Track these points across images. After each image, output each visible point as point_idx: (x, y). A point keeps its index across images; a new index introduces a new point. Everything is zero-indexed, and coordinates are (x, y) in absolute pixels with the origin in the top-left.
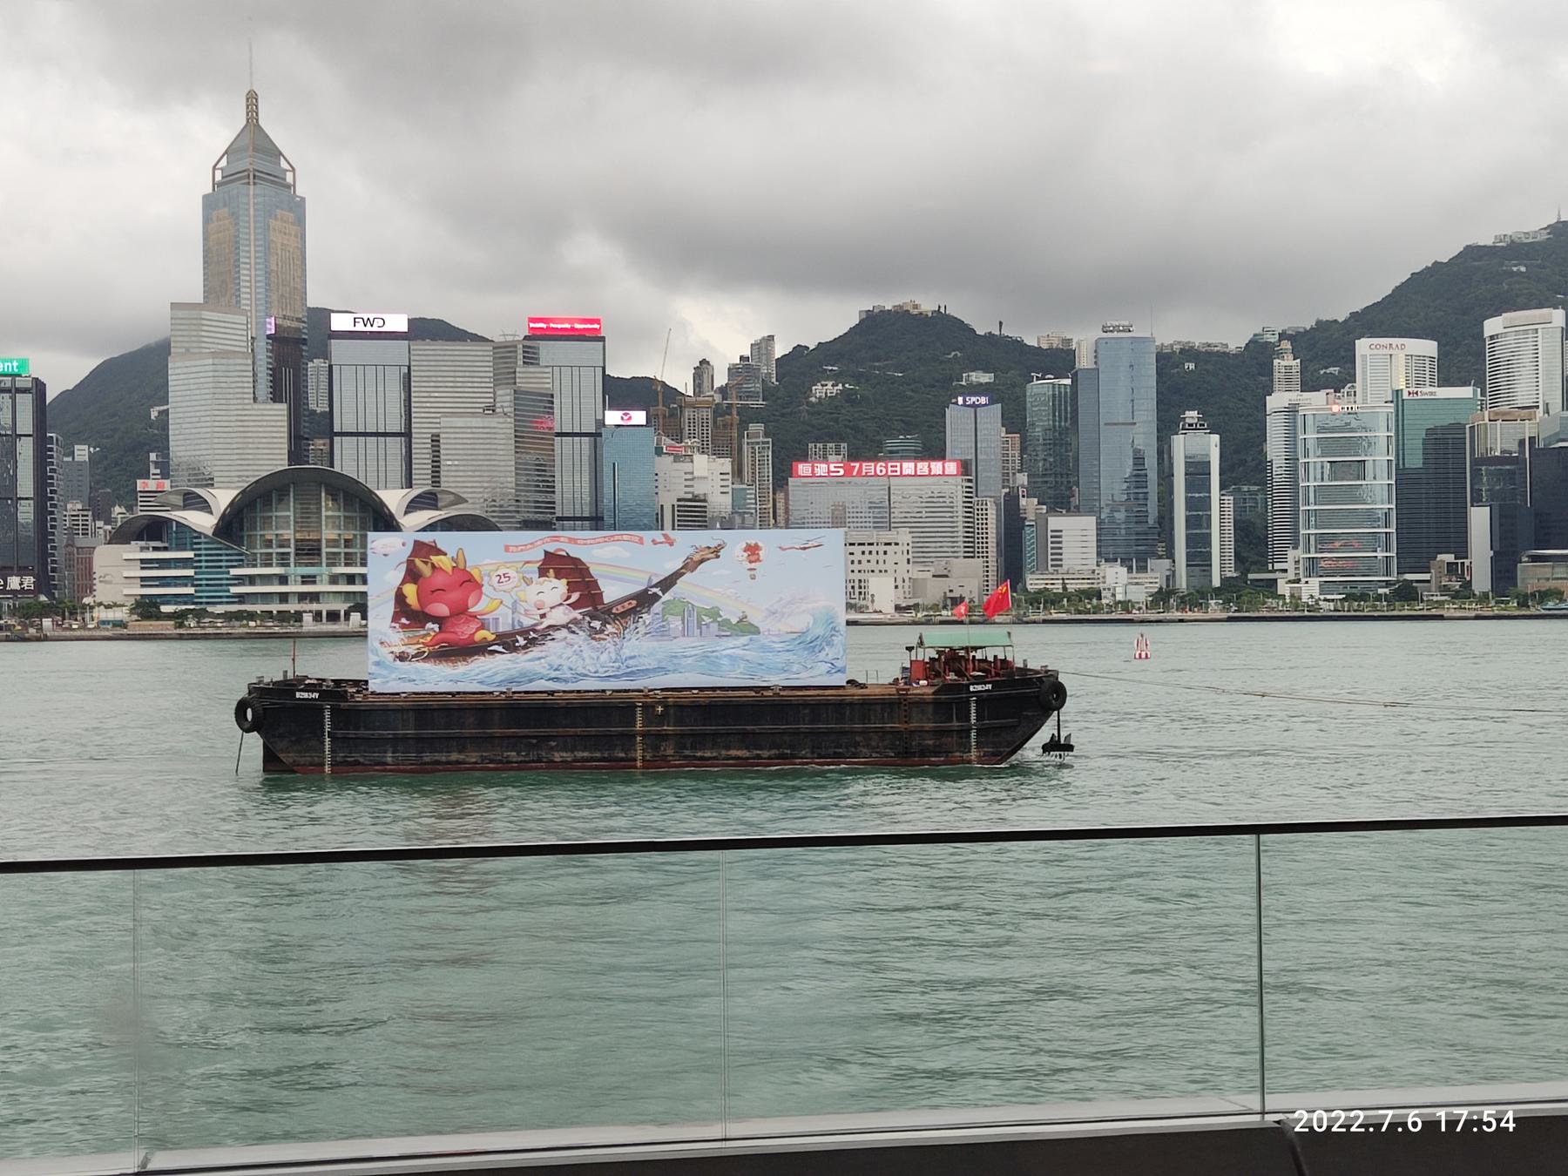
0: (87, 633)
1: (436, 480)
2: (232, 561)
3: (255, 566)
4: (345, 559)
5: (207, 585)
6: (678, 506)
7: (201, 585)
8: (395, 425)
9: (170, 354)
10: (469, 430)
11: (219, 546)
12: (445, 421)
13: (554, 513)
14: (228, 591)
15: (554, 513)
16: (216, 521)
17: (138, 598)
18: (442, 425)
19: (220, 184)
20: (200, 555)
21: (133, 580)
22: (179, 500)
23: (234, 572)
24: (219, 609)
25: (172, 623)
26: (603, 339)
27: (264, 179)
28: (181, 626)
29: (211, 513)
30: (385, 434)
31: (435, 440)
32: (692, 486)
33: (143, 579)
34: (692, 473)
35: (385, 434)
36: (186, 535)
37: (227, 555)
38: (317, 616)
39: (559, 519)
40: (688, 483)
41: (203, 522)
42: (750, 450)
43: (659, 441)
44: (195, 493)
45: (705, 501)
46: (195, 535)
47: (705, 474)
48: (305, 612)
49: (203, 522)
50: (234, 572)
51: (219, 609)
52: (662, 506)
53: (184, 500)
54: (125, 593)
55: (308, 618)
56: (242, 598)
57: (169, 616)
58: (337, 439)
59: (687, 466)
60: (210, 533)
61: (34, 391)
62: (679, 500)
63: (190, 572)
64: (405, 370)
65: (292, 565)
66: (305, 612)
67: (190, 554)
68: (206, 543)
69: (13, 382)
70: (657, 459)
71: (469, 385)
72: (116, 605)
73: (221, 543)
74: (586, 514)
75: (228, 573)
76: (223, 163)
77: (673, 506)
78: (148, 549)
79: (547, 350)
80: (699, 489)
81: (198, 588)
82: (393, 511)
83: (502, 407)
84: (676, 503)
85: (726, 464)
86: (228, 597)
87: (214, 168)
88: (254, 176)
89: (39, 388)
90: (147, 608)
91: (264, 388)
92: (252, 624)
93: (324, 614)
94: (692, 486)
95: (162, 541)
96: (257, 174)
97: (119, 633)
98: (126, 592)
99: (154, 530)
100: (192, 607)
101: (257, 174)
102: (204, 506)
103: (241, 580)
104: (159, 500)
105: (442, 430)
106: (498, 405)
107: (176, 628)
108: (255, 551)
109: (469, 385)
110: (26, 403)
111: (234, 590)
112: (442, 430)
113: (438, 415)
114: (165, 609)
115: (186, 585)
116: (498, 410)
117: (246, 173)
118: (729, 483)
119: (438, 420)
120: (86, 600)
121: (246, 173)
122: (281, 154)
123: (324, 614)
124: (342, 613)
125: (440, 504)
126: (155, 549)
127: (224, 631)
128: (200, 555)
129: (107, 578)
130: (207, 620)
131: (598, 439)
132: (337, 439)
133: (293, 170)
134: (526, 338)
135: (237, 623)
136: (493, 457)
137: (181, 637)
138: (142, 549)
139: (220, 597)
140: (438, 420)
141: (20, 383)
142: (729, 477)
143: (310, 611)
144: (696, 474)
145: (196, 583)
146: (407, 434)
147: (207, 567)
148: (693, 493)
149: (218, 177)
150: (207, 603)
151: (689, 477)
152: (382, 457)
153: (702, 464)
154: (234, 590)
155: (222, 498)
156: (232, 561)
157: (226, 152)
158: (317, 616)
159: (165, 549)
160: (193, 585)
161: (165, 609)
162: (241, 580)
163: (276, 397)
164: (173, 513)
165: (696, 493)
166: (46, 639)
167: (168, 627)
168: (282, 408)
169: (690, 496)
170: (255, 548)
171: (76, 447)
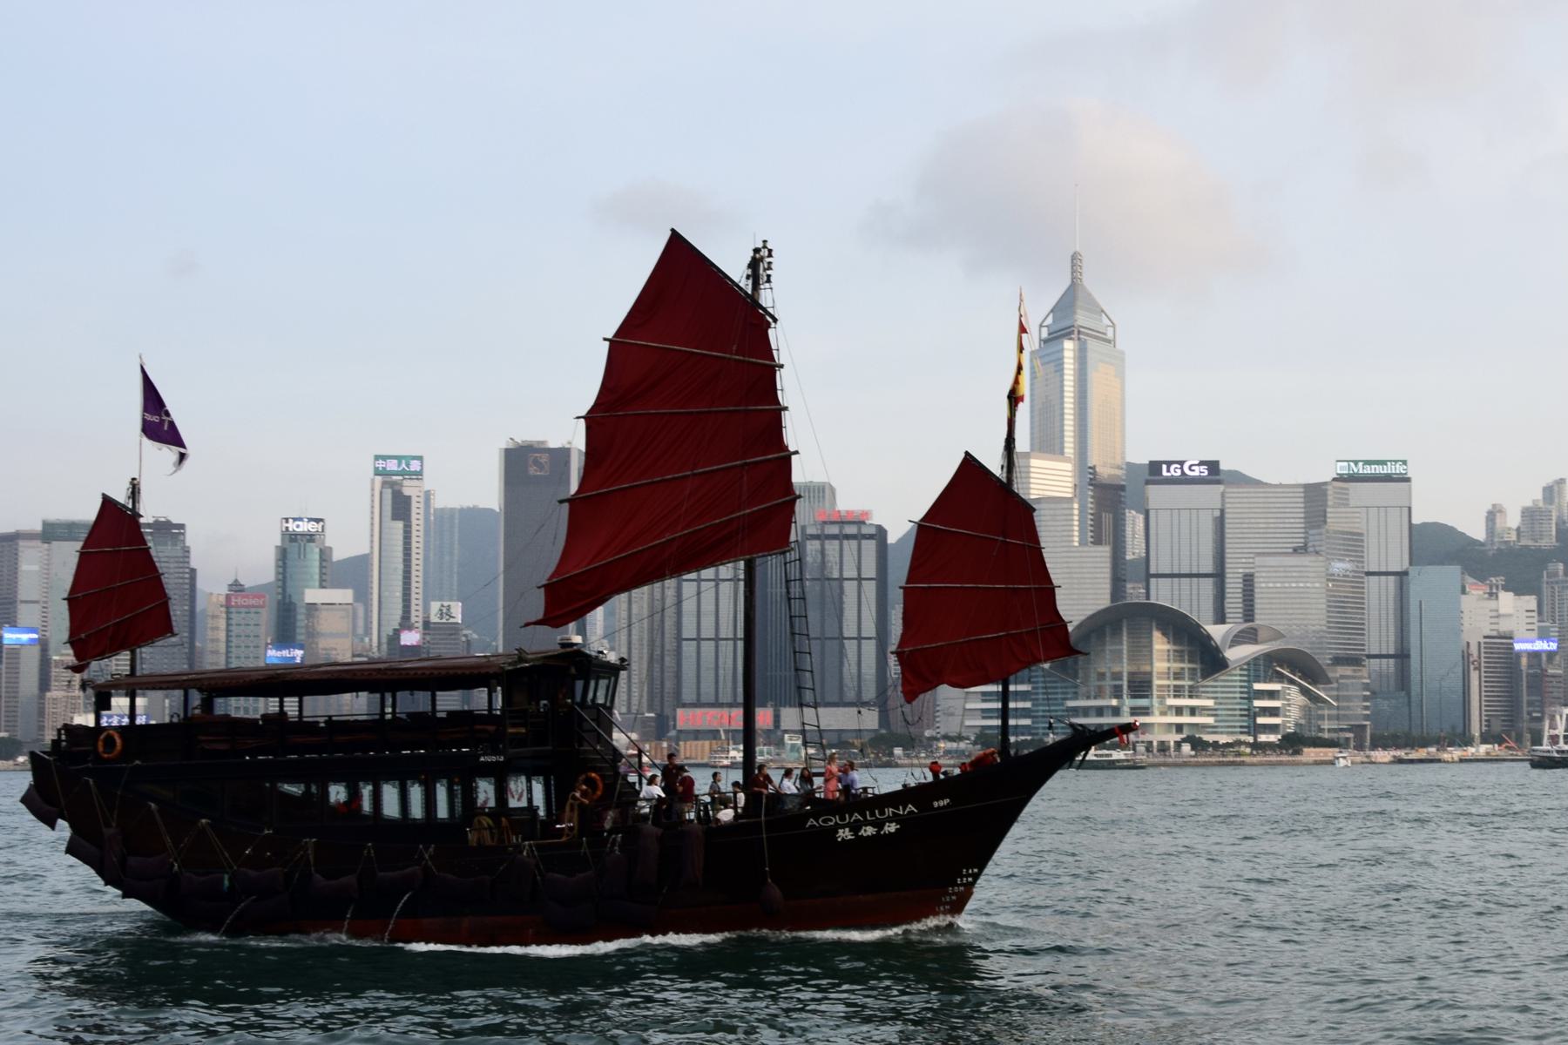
4: (1175, 691)
6: (1485, 643)
8: (1208, 566)
10: (1282, 569)
12: (1259, 560)
13: (1363, 650)
15: (1363, 650)
18: (1257, 564)
19: (1046, 341)
20: (1037, 688)
26: (1408, 480)
27: (1087, 335)
30: (1198, 576)
31: (1248, 581)
32: (1498, 623)
34: (1497, 611)
35: (1198, 576)
39: (1370, 656)
40: (1494, 620)
42: (1550, 590)
43: (1463, 579)
45: (1511, 638)
47: (1511, 611)
52: (1468, 643)
58: (1153, 581)
59: (1492, 604)
62: (1485, 637)
64: (1217, 513)
69: (859, 529)
70: (1463, 596)
71: (1281, 525)
74: (1392, 652)
76: (1049, 321)
77: (1479, 643)
79: (1357, 490)
80: (1504, 626)
83: (1314, 546)
84: (1482, 640)
85: (1530, 602)
88: (1079, 332)
89: (881, 533)
94: (1498, 623)
101: (1082, 330)
105: (1258, 569)
106: (1310, 544)
109: (1281, 525)
110: (870, 547)
112: (1258, 569)
113: (1252, 555)
118: (1535, 620)
119: (1251, 560)
122: (1103, 311)
128: (1037, 688)
131: (1405, 577)
132: (1153, 581)
133: (1114, 326)
134: (1334, 479)
136: (1306, 596)
140: (1251, 560)
141: (865, 530)
142: (1535, 614)
144: (1502, 611)
146: (1219, 576)
148: (1497, 630)
149: (1045, 334)
151: (1494, 614)
152: (1195, 597)
153: (1507, 600)
157: (1052, 311)
165: (1501, 630)
169: (1494, 633)
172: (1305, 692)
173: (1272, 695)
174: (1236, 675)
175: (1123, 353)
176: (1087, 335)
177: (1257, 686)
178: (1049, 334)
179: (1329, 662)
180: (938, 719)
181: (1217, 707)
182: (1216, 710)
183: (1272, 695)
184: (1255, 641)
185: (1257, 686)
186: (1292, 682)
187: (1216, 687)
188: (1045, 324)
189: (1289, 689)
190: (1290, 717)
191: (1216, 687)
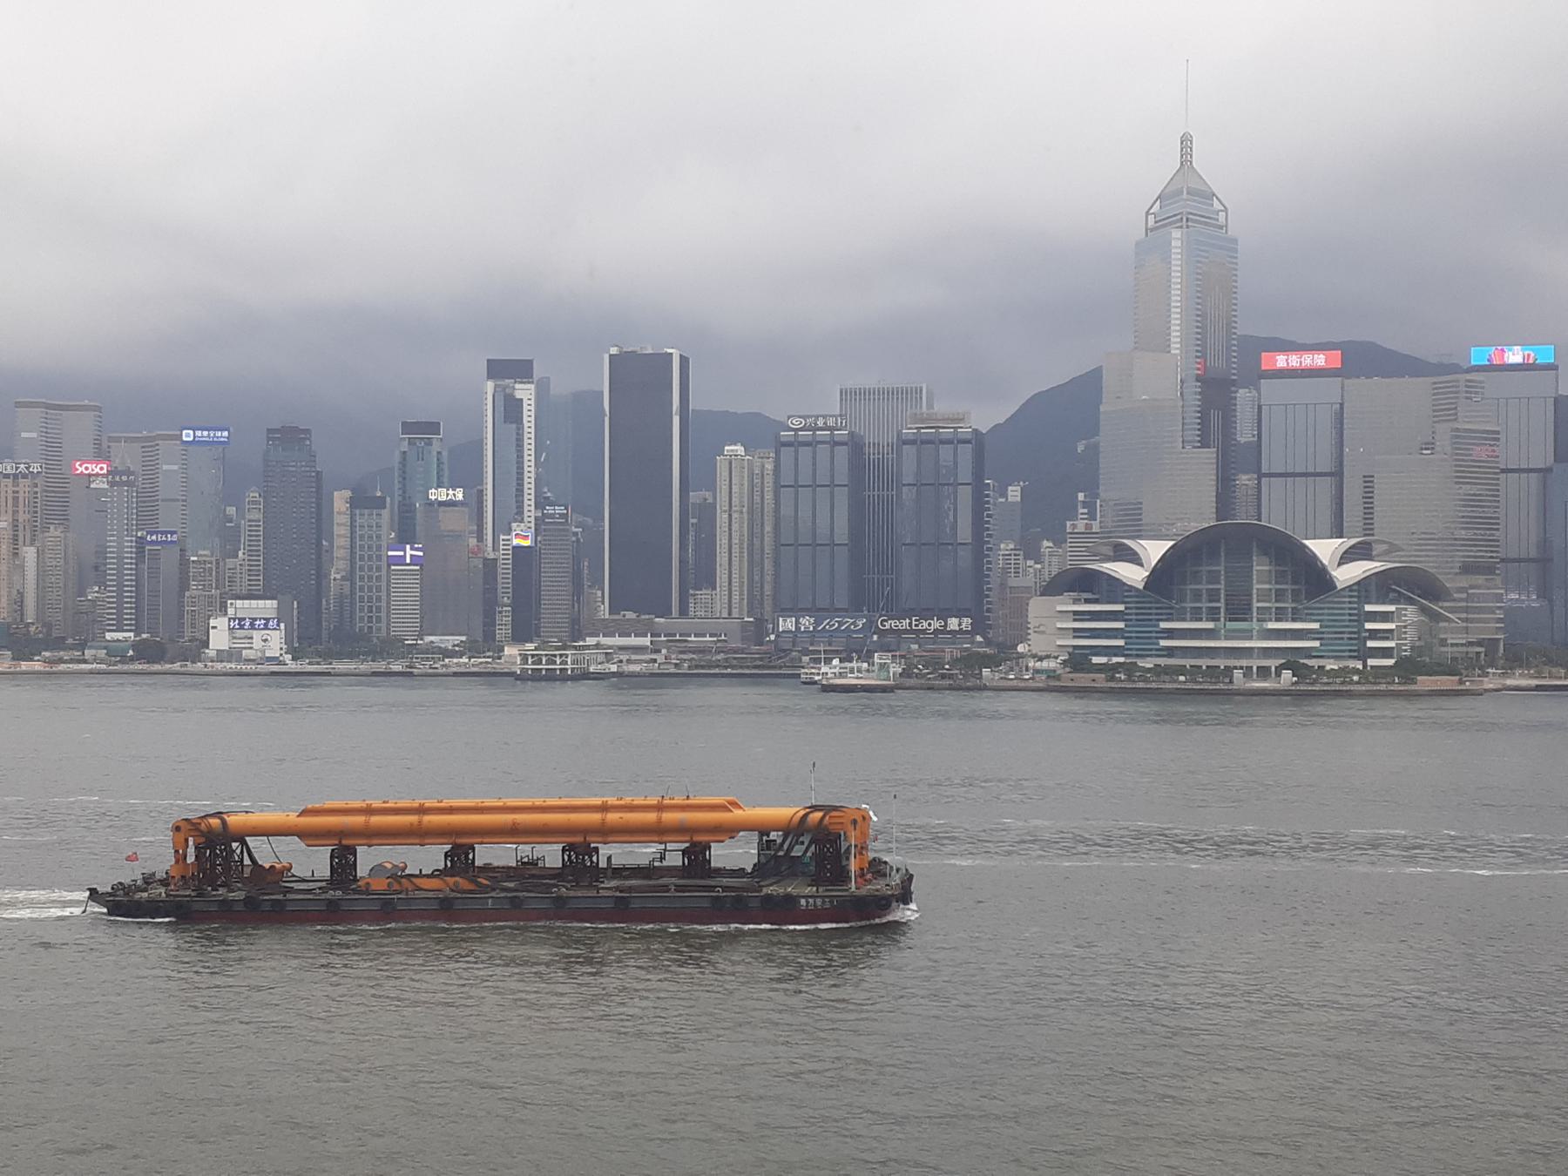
0: (1022, 684)
1: (1368, 528)
2: (1161, 614)
3: (1184, 620)
5: (1137, 638)
7: (1131, 638)
9: (1101, 403)
11: (1149, 599)
14: (1158, 644)
16: (1147, 574)
17: (1071, 650)
21: (1063, 632)
22: (1108, 551)
23: (1163, 625)
24: (1148, 664)
25: (1103, 676)
27: (1196, 221)
28: (1112, 679)
29: (1142, 565)
33: (1075, 630)
36: (1115, 588)
37: (1157, 608)
38: (1248, 671)
41: (1133, 575)
44: (1124, 544)
46: (1126, 588)
48: (1236, 668)
49: (1133, 575)
50: (1163, 625)
51: (1148, 664)
53: (1115, 552)
54: (1058, 643)
55: (1238, 674)
56: (1171, 652)
57: (1101, 668)
60: (1141, 587)
61: (973, 442)
63: (1121, 625)
65: (1222, 619)
66: (1236, 668)
67: (1120, 607)
68: (1137, 596)
72: (1048, 657)
73: (1150, 596)
75: (1158, 626)
78: (1080, 600)
81: (1128, 640)
82: (1325, 562)
86: (1157, 650)
87: (1147, 213)
90: (1078, 661)
91: (1193, 434)
92: (1182, 678)
93: (1255, 669)
95: (1094, 594)
96: (1190, 216)
97: (1053, 686)
98: (1059, 643)
99: (1086, 583)
100: (1121, 660)
101: (1190, 216)
102: (1134, 558)
103: (1171, 634)
104: (1091, 550)
107: (1107, 681)
108: (1183, 605)
111: (1163, 643)
114: (1096, 660)
115: (1116, 638)
116: (1438, 449)
117: (1179, 217)
120: (1020, 648)
121: (1179, 217)
122: (1214, 195)
123: (1255, 669)
124: (1273, 669)
125: (1374, 553)
126: (1087, 601)
127: (1154, 685)
129: (1042, 628)
130: (1138, 674)
135: (1167, 678)
137: (1111, 691)
138: (1076, 601)
139: (1151, 650)
143: (1241, 668)
145: (1126, 635)
147: (1137, 620)
150: (1137, 656)
154: (1163, 643)
155: (1154, 550)
156: (1161, 614)
158: (1248, 671)
159: (1096, 601)
160: (1123, 638)
161: (1096, 660)
162: (1171, 634)
163: (1204, 444)
164: (1104, 565)
166: (985, 688)
167: (1100, 680)
168: (1209, 454)
170: (1184, 601)
171: (1019, 499)
172: (1424, 610)
173: (1385, 617)
174: (1345, 597)
175: (1235, 241)
176: (1196, 221)
177: (1368, 608)
178: (1156, 222)
179: (1458, 571)
180: (1029, 637)
181: (1321, 630)
182: (1323, 633)
183: (1385, 617)
184: (1370, 558)
185: (1368, 608)
186: (1411, 601)
187: (1323, 609)
188: (1152, 211)
189: (1406, 609)
190: (1406, 639)
191: (1323, 609)
